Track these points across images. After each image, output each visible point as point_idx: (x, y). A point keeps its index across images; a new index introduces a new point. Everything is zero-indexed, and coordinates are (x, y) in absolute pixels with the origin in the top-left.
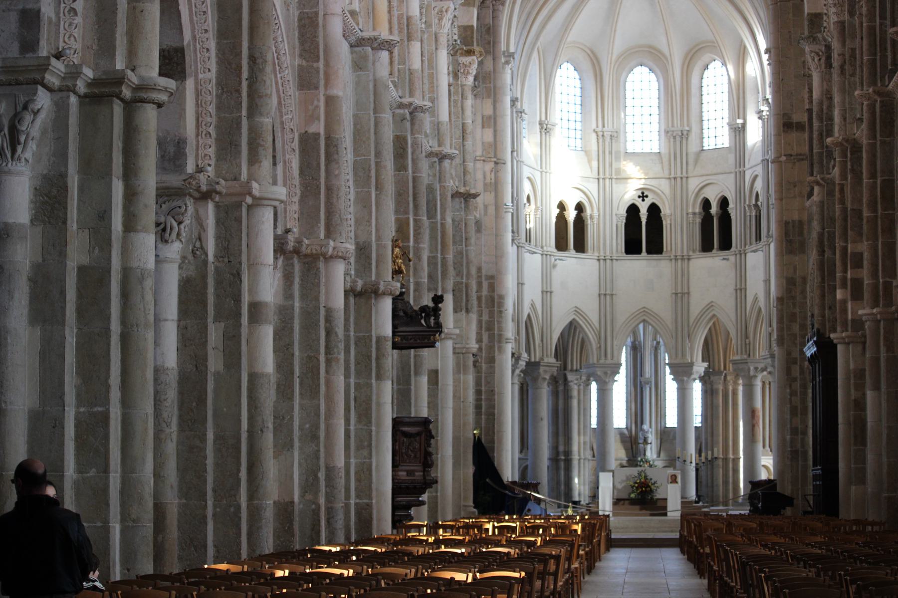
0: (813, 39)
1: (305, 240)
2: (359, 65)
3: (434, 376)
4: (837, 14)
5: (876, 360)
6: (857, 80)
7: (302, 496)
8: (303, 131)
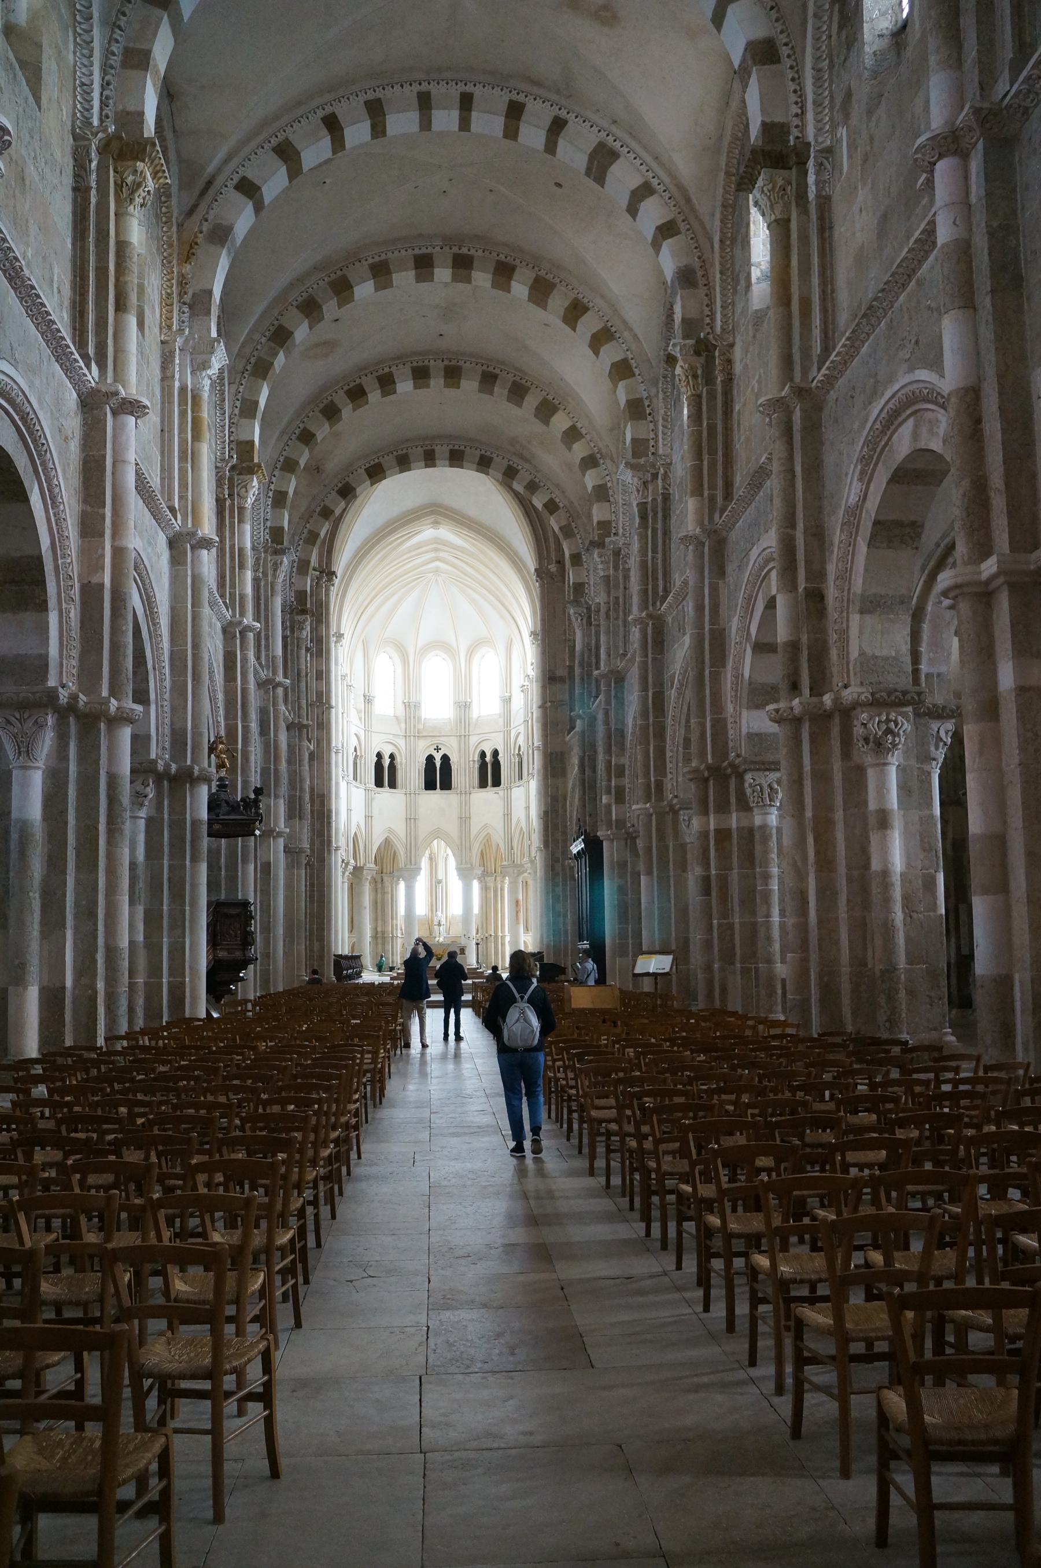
0: (576, 602)
1: (81, 695)
2: (177, 559)
3: (266, 869)
4: (604, 570)
5: (649, 849)
6: (621, 623)
7: (76, 981)
8: (86, 582)
